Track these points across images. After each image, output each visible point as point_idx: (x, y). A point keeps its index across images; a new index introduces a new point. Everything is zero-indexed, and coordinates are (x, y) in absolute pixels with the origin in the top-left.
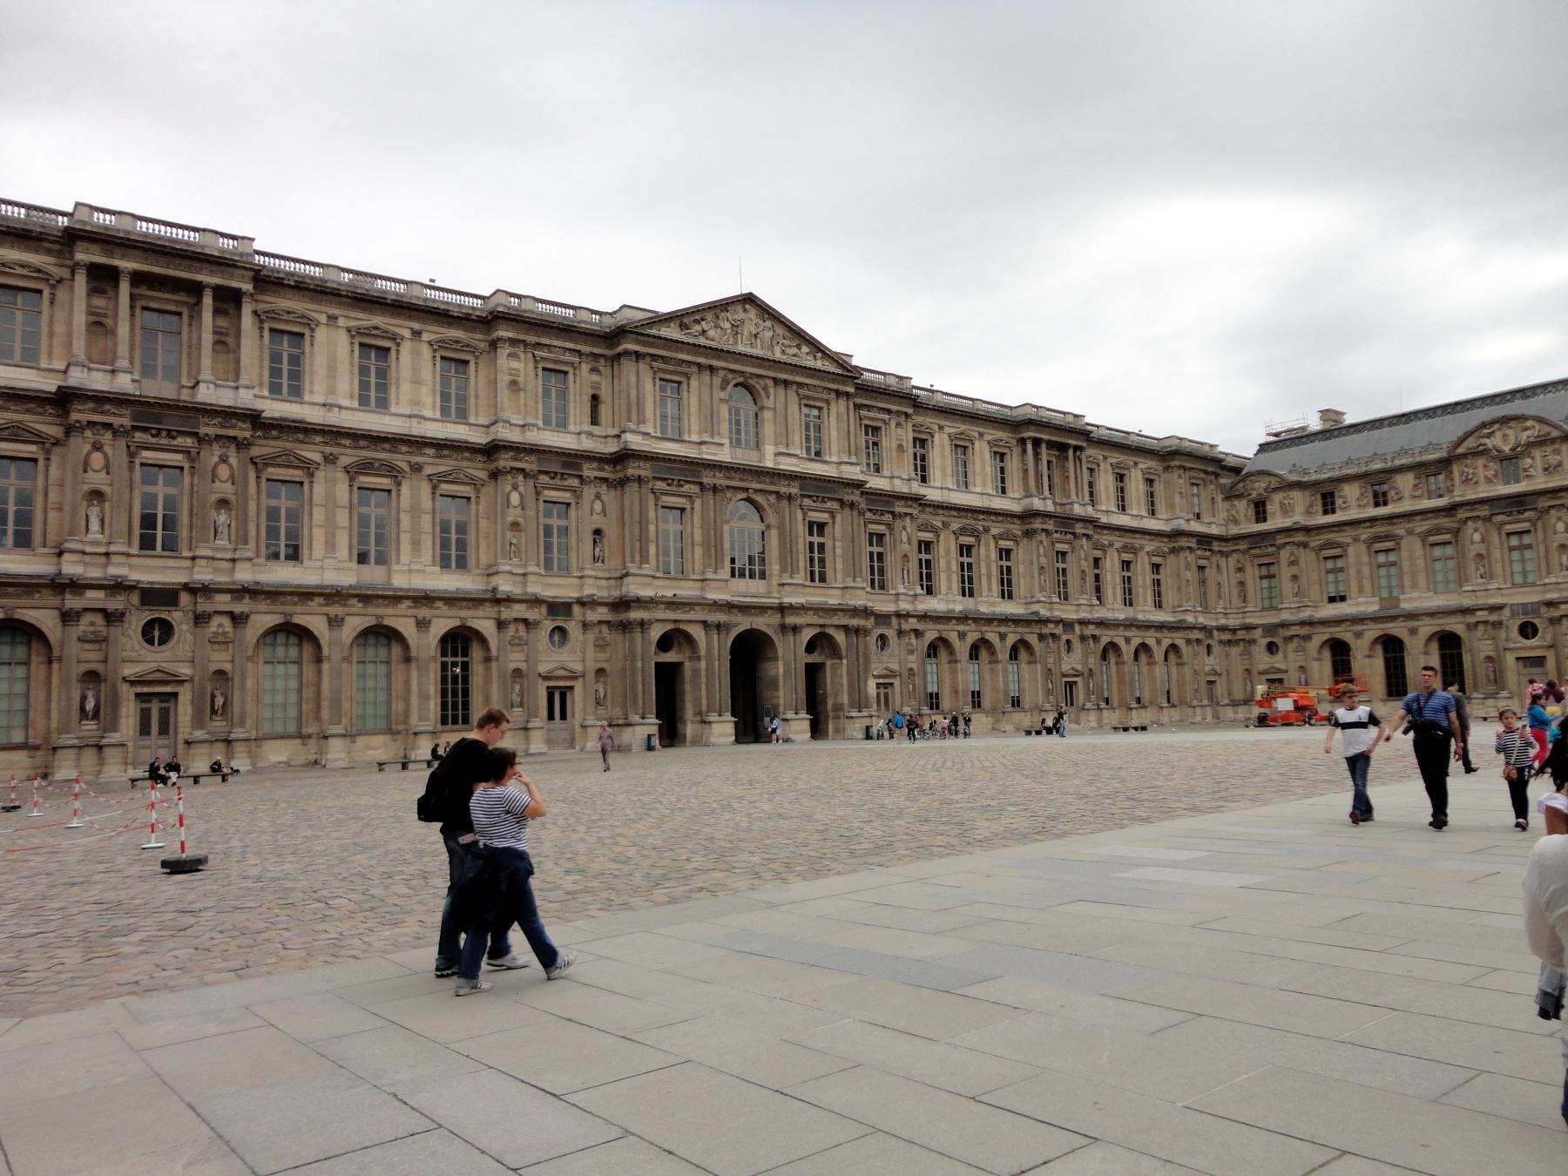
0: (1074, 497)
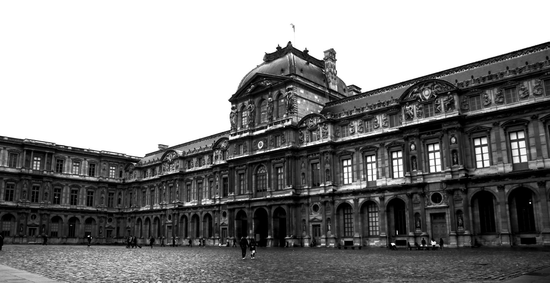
0: (45, 169)
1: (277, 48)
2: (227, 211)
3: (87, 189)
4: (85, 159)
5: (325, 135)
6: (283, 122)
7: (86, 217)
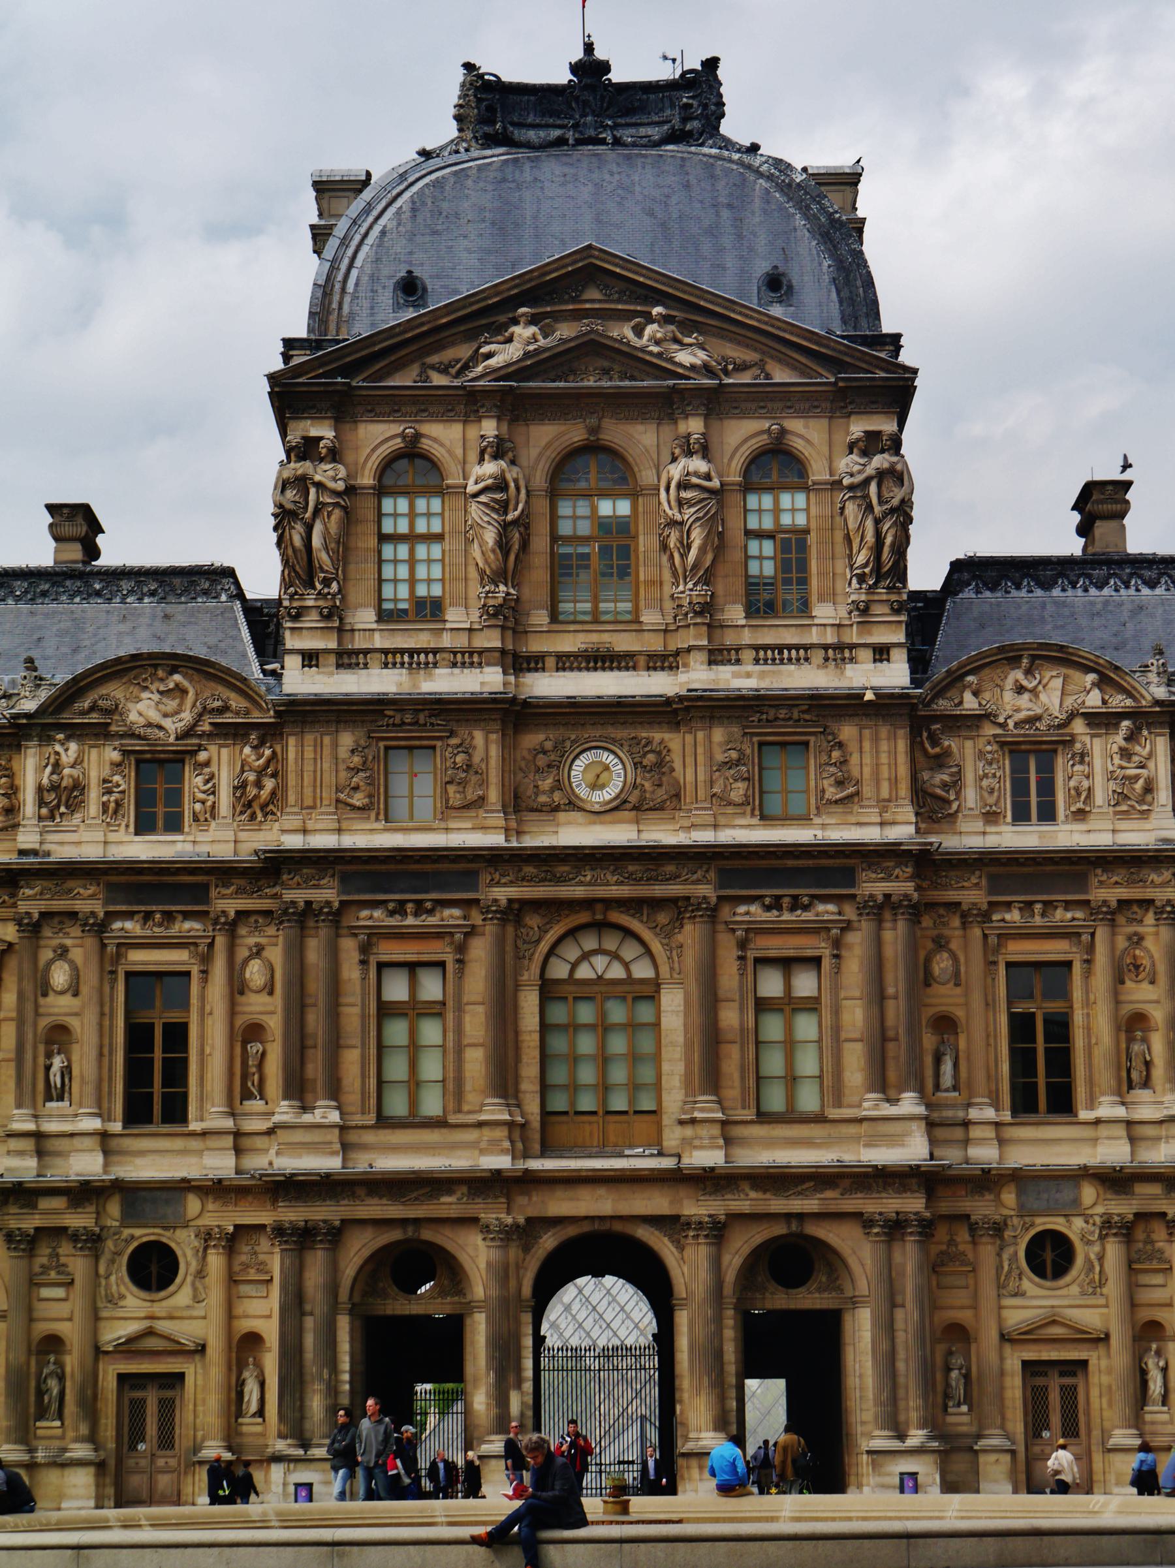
1: (575, 68)
2: (184, 1244)
5: (1133, 798)
6: (839, 652)
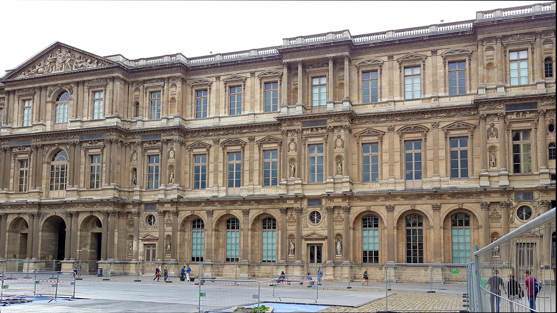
3: (449, 129)
4: (434, 52)
7: (449, 206)
